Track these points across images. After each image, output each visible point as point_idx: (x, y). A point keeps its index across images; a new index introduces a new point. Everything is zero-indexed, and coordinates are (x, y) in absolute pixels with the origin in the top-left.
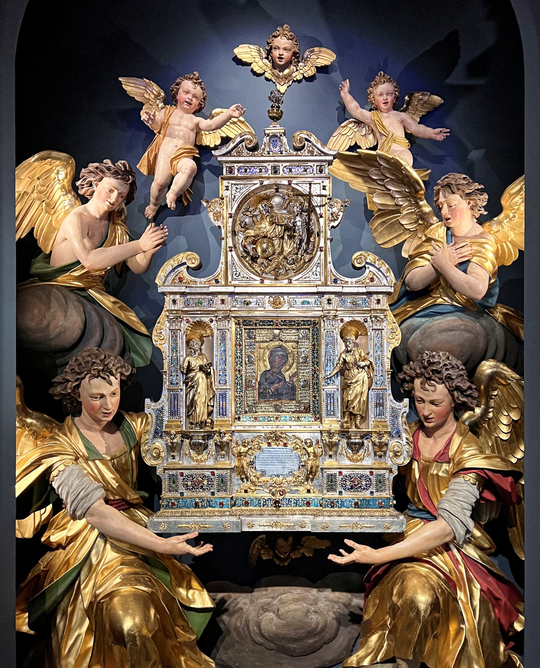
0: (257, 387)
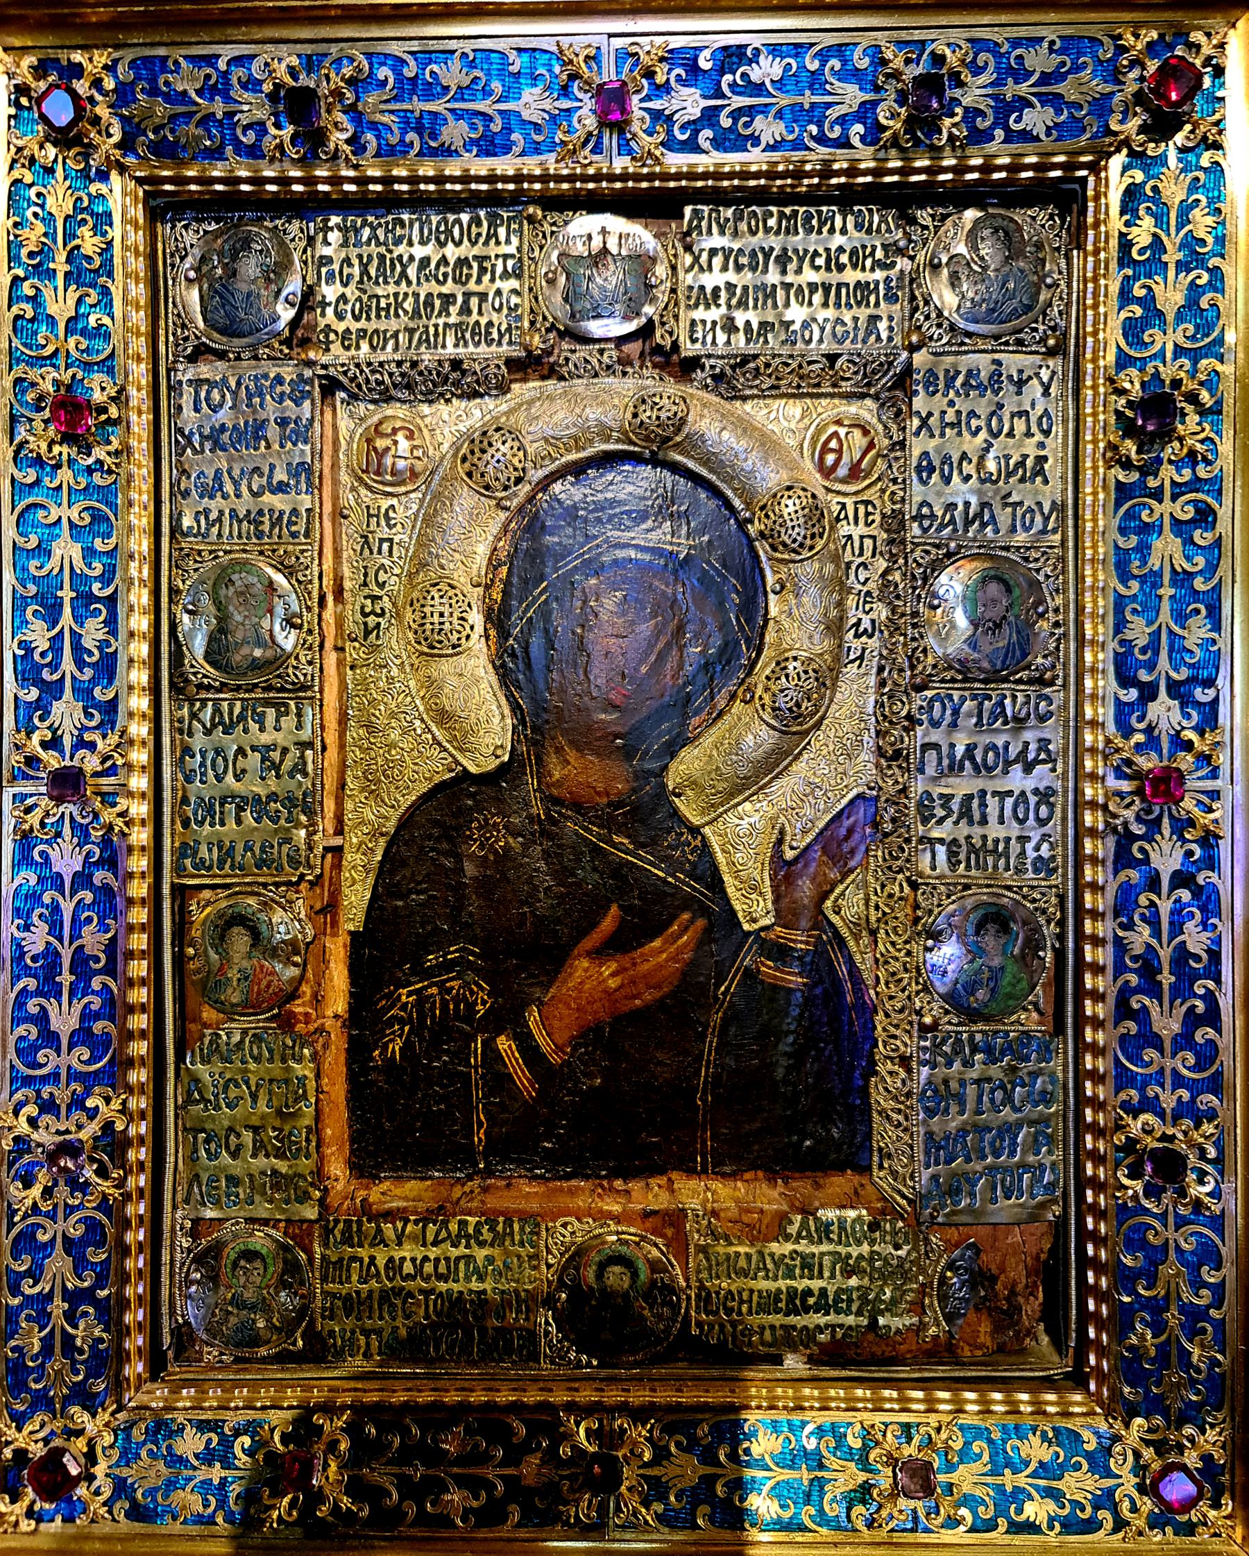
0: (338, 1003)
